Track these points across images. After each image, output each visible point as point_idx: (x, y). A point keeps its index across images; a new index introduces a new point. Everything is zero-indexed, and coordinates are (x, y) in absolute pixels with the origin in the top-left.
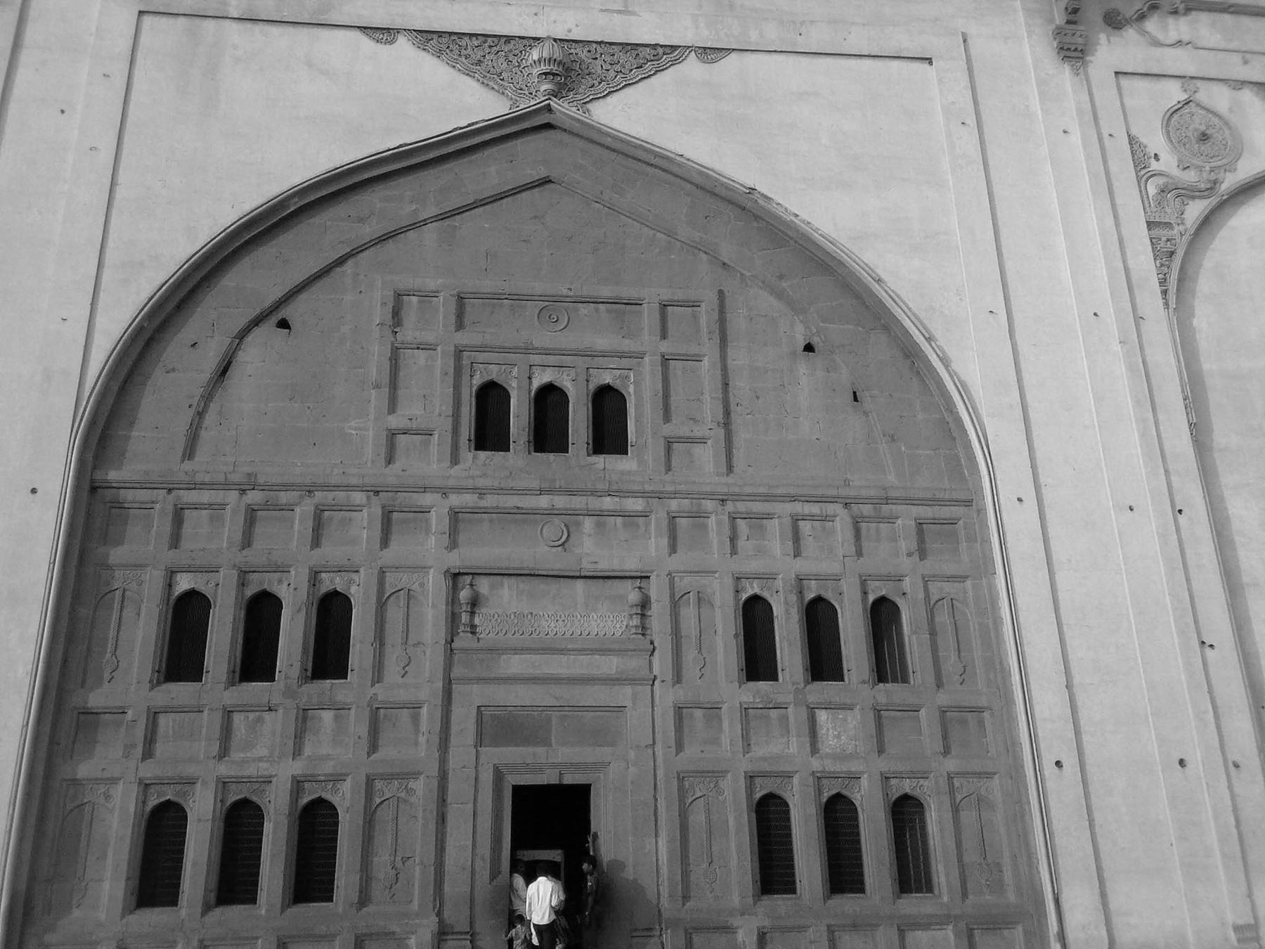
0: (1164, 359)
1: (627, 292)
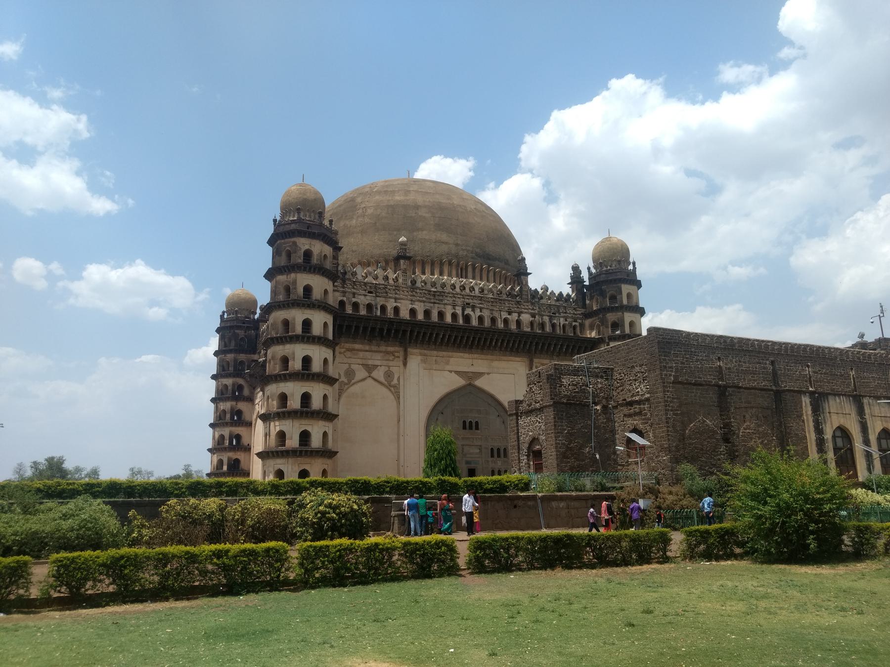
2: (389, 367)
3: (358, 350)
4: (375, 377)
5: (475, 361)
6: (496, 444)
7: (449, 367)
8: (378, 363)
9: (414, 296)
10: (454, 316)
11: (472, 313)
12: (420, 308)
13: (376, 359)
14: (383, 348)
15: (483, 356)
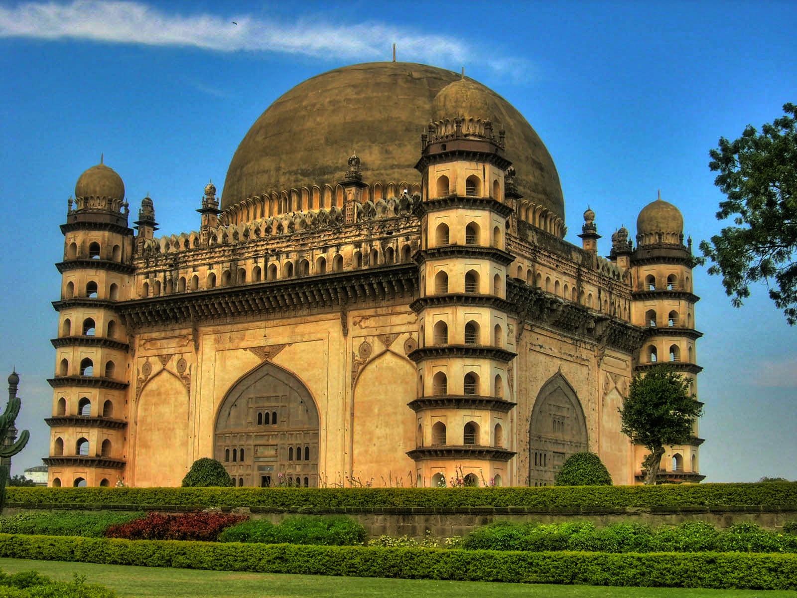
0: (349, 400)
1: (277, 395)
2: (182, 354)
3: (156, 339)
5: (268, 331)
6: (295, 442)
7: (243, 344)
8: (172, 351)
9: (212, 257)
10: (258, 271)
11: (276, 263)
12: (218, 270)
13: (170, 347)
14: (177, 333)
15: (285, 321)
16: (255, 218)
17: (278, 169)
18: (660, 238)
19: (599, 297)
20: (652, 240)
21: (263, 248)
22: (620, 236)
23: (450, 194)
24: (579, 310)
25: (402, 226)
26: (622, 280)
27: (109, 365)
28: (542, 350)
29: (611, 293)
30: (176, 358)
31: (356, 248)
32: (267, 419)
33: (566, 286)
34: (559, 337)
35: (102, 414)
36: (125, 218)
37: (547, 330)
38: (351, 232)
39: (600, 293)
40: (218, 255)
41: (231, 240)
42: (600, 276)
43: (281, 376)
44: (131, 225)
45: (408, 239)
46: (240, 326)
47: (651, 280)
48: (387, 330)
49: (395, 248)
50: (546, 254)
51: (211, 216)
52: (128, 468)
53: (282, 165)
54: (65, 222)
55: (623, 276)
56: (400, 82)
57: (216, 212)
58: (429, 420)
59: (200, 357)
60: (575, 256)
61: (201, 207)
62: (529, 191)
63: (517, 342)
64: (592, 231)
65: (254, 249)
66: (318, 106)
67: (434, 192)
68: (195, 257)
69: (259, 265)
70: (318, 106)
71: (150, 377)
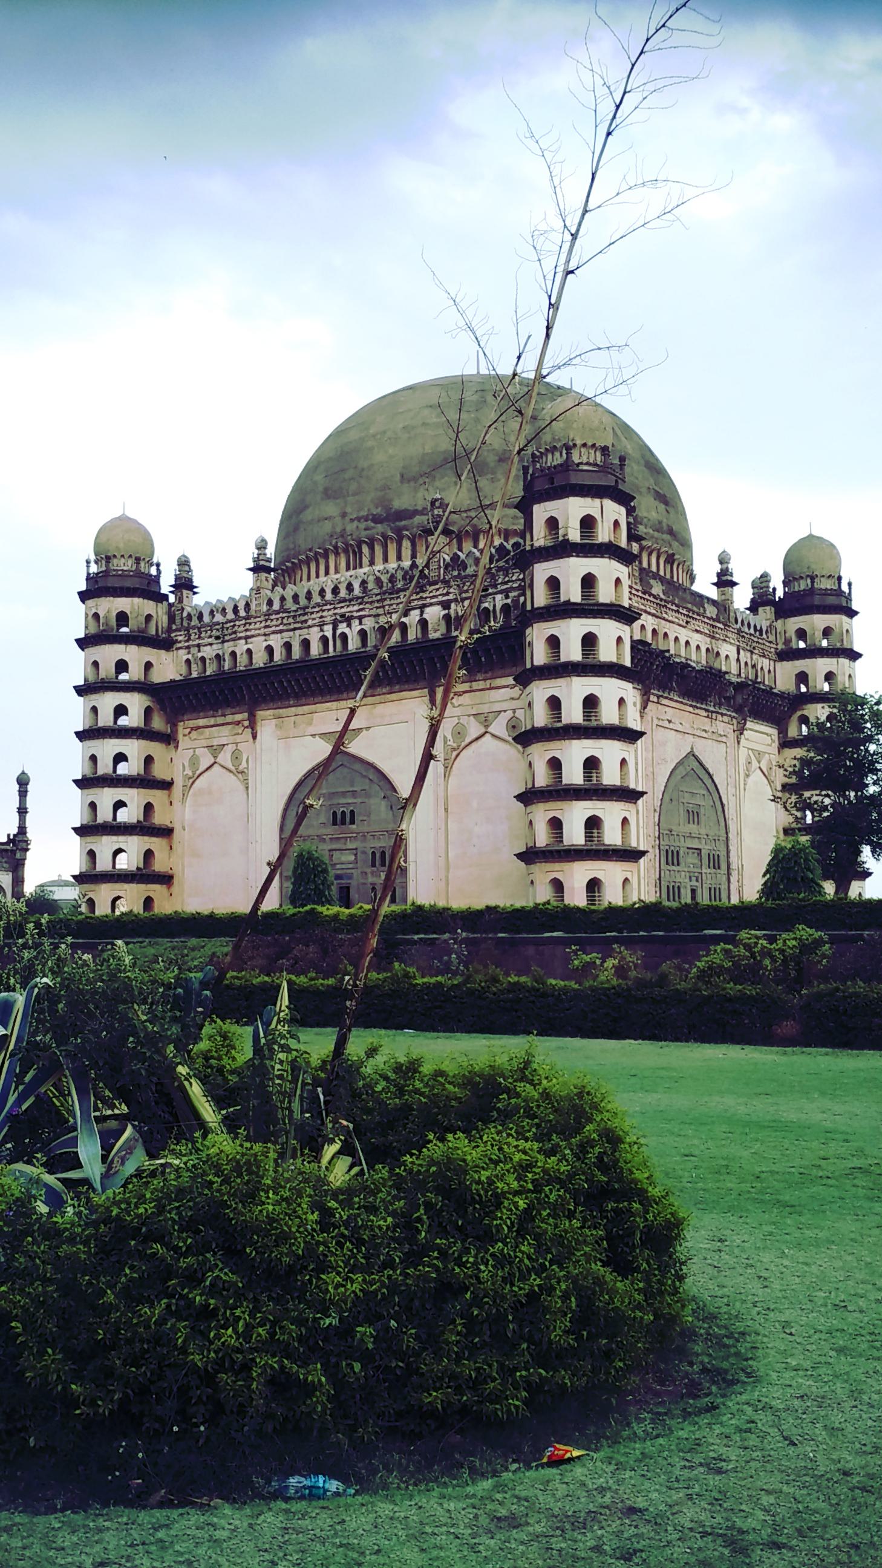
0: (441, 794)
4: (222, 763)
8: (224, 741)
10: (324, 640)
11: (347, 631)
12: (276, 642)
13: (222, 735)
16: (318, 576)
17: (344, 515)
18: (812, 582)
19: (738, 660)
20: (804, 585)
21: (331, 613)
22: (761, 584)
23: (561, 538)
24: (716, 675)
25: (500, 581)
26: (764, 636)
27: (149, 760)
28: (671, 726)
29: (752, 653)
30: (230, 748)
31: (444, 609)
32: (342, 819)
33: (698, 647)
34: (691, 709)
35: (142, 819)
36: (156, 580)
37: (677, 701)
38: (437, 590)
39: (738, 653)
40: (274, 623)
41: (290, 604)
42: (739, 632)
43: (357, 766)
44: (165, 589)
45: (507, 597)
46: (306, 708)
47: (801, 634)
48: (485, 709)
49: (491, 609)
50: (674, 608)
51: (264, 575)
52: (176, 880)
53: (349, 510)
54: (84, 588)
55: (767, 631)
56: (490, 398)
57: (268, 570)
58: (542, 813)
59: (258, 746)
60: (711, 611)
61: (251, 565)
62: (651, 531)
63: (642, 717)
64: (729, 578)
65: (319, 615)
66: (389, 434)
67: (540, 537)
68: (247, 626)
69: (326, 634)
70: (389, 434)
71: (198, 772)
